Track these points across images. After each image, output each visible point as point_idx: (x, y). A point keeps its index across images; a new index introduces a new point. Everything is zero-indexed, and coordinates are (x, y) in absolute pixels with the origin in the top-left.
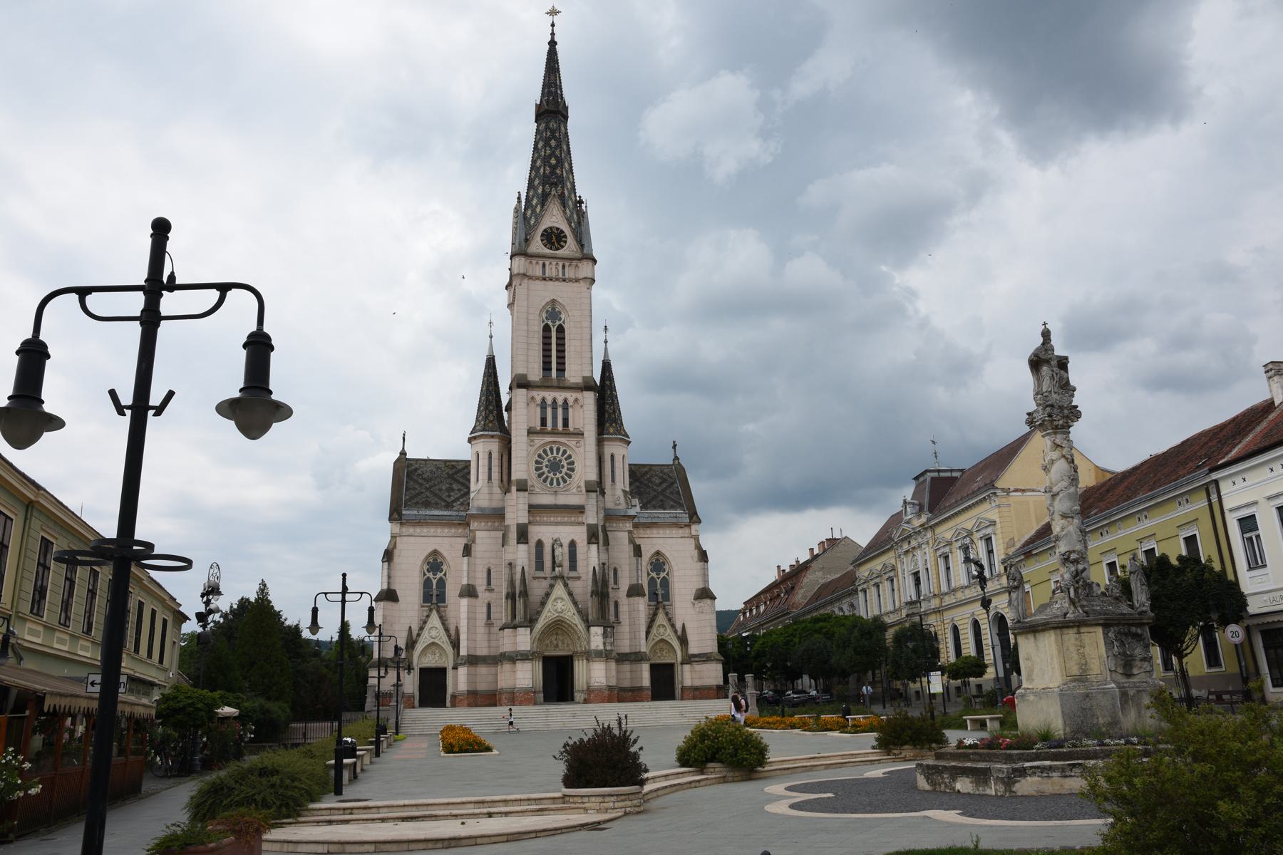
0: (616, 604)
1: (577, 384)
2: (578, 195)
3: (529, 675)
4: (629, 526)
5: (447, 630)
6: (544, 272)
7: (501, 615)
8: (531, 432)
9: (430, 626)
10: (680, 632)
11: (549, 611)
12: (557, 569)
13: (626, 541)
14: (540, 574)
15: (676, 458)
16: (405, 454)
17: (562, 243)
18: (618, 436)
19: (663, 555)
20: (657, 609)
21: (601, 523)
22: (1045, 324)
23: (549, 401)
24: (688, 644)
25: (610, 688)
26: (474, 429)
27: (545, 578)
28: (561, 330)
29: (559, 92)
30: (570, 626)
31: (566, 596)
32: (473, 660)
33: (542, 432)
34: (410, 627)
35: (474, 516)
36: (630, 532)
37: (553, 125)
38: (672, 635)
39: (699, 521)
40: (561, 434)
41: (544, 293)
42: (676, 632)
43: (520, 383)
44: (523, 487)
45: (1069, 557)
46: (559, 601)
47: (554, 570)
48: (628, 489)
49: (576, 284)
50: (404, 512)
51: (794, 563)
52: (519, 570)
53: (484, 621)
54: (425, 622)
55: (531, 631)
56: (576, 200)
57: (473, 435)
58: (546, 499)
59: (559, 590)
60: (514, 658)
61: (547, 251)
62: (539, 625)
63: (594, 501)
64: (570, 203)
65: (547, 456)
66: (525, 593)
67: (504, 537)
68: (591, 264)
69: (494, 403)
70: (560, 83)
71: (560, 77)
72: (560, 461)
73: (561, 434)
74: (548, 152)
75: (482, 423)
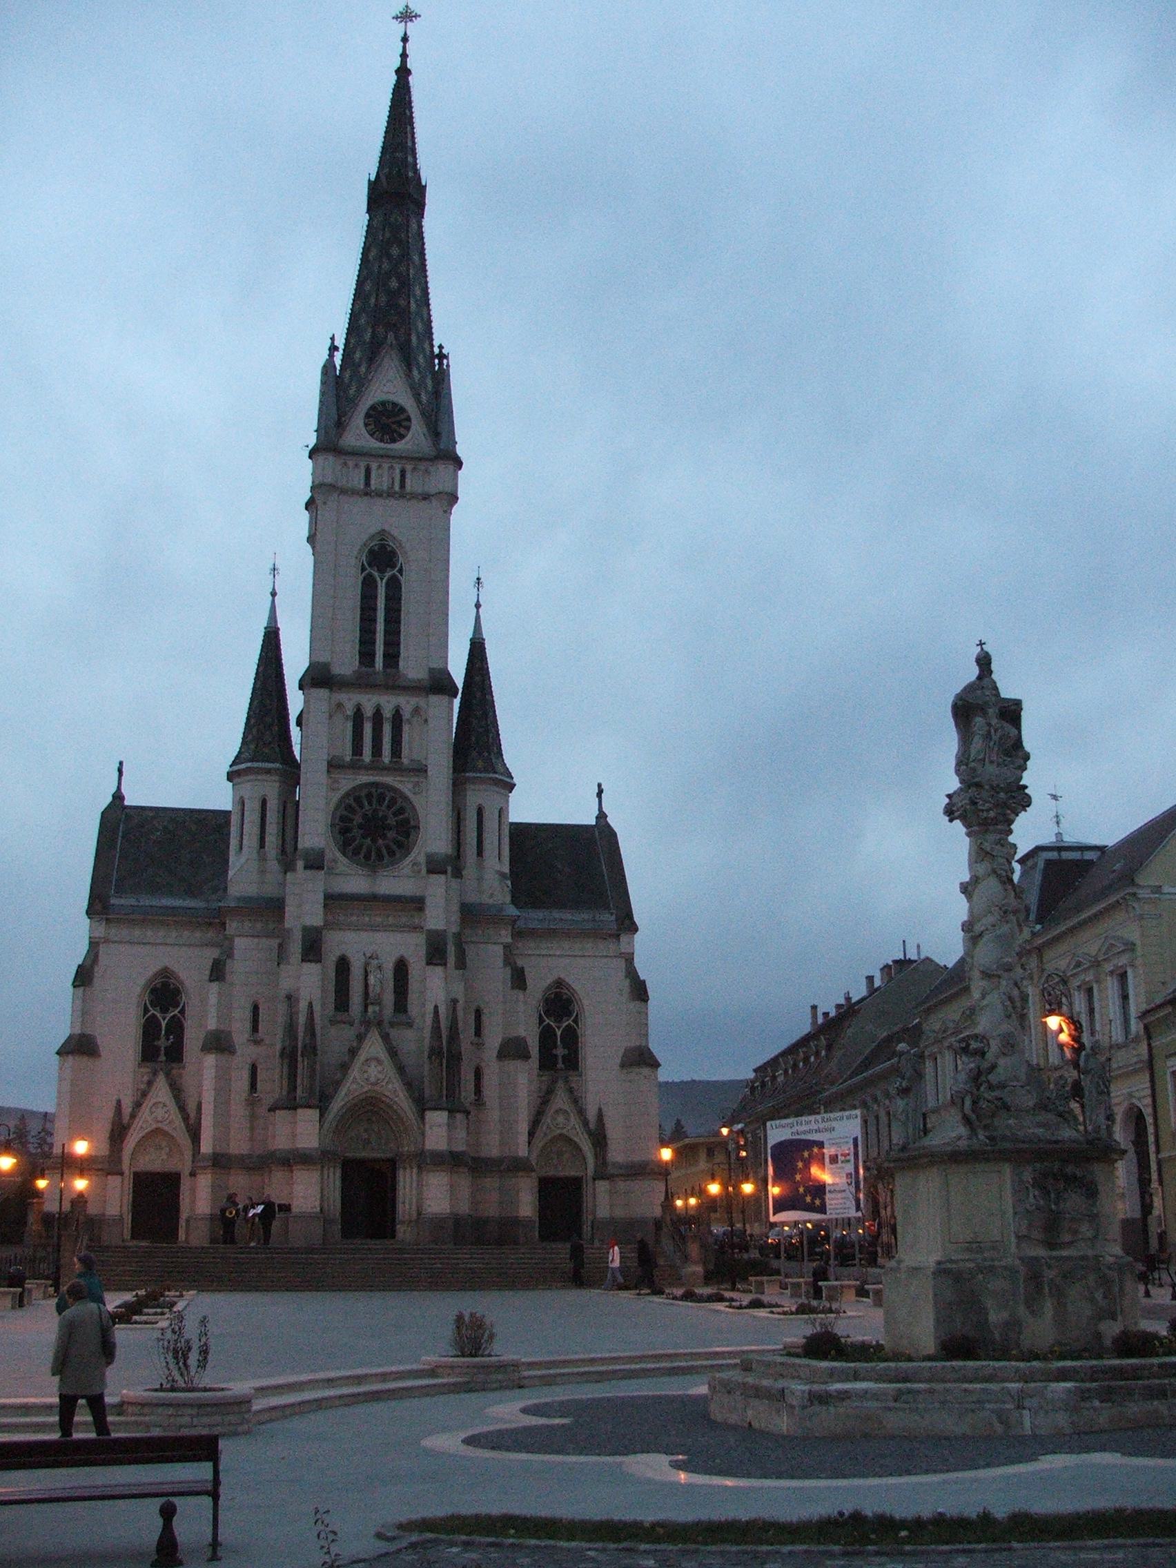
0: (478, 1074)
2: (436, 343)
3: (314, 1192)
5: (182, 1108)
6: (367, 483)
7: (272, 1083)
9: (153, 1101)
10: (592, 1126)
12: (370, 1009)
13: (500, 963)
14: (341, 1016)
15: (602, 816)
18: (491, 775)
19: (568, 987)
20: (554, 1082)
21: (454, 929)
22: (981, 644)
23: (368, 711)
24: (606, 1144)
25: (457, 1221)
26: (237, 757)
28: (394, 587)
29: (410, 159)
30: (390, 1107)
31: (382, 1054)
32: (220, 1162)
33: (355, 766)
34: (119, 1102)
36: (507, 947)
37: (396, 218)
38: (579, 1128)
39: (634, 928)
42: (585, 1123)
43: (316, 678)
44: (316, 862)
45: (968, 1045)
46: (373, 1064)
47: (366, 1007)
48: (506, 870)
49: (423, 504)
51: (842, 1001)
52: (303, 1005)
53: (245, 1095)
54: (144, 1094)
55: (321, 1116)
56: (432, 351)
57: (235, 768)
58: (355, 882)
59: (373, 1046)
60: (292, 1160)
61: (374, 444)
62: (337, 1104)
63: (440, 891)
65: (362, 807)
66: (311, 1049)
67: (282, 950)
68: (451, 467)
70: (414, 143)
71: (413, 134)
72: (385, 818)
74: (386, 266)
75: (252, 747)
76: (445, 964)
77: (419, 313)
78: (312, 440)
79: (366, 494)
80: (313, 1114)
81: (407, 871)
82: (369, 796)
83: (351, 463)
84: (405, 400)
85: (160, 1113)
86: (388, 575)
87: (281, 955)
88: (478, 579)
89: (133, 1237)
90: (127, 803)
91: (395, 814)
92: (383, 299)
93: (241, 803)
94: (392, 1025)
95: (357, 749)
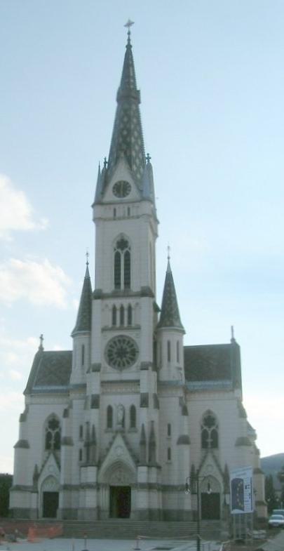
0: (169, 451)
1: (138, 292)
2: (146, 154)
4: (180, 393)
6: (115, 215)
8: (104, 330)
10: (223, 470)
13: (177, 404)
14: (109, 429)
15: (233, 340)
20: (207, 453)
23: (118, 307)
27: (112, 432)
28: (127, 255)
31: (123, 445)
33: (113, 329)
36: (181, 398)
42: (220, 470)
44: (97, 369)
52: (91, 427)
54: (45, 462)
58: (113, 375)
61: (117, 199)
62: (105, 465)
66: (94, 443)
78: (92, 200)
79: (114, 219)
80: (94, 469)
82: (119, 341)
84: (127, 178)
85: (51, 469)
86: (125, 251)
87: (85, 408)
89: (44, 516)
92: (121, 140)
93: (75, 346)
94: (129, 432)
95: (114, 322)
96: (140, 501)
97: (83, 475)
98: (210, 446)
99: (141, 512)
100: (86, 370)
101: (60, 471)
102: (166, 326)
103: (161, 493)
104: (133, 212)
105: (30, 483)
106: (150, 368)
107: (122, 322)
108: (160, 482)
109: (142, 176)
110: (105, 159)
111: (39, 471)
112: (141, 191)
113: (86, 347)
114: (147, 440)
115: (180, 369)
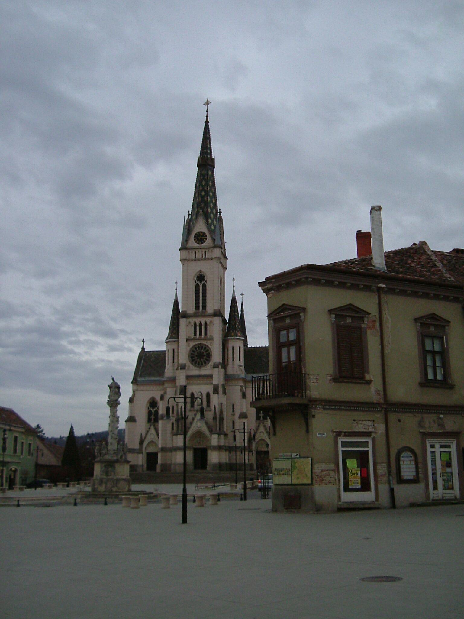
0: (233, 423)
2: (218, 208)
6: (195, 257)
8: (188, 340)
11: (194, 427)
13: (239, 391)
14: (192, 409)
16: (144, 349)
17: (204, 240)
20: (260, 423)
23: (198, 323)
27: (195, 411)
28: (204, 286)
33: (194, 339)
34: (141, 434)
35: (166, 381)
36: (241, 386)
40: (203, 339)
41: (196, 268)
44: (183, 367)
50: (138, 379)
52: (180, 408)
54: (148, 431)
61: (196, 245)
64: (212, 216)
65: (197, 350)
69: (176, 324)
70: (210, 145)
72: (203, 353)
73: (203, 339)
74: (201, 188)
76: (218, 393)
77: (211, 201)
78: (180, 246)
79: (195, 260)
81: (209, 367)
83: (190, 252)
85: (152, 436)
86: (202, 283)
88: (234, 278)
90: (146, 350)
91: (206, 352)
92: (200, 199)
96: (214, 457)
97: (174, 441)
98: (262, 419)
99: (215, 465)
100: (176, 368)
101: (158, 438)
102: (231, 336)
103: (227, 453)
104: (208, 255)
105: (137, 446)
106: (220, 366)
107: (200, 334)
108: (227, 444)
109: (215, 227)
110: (189, 212)
111: (143, 438)
112: (214, 240)
113: (176, 351)
114: (218, 416)
115: (240, 366)
